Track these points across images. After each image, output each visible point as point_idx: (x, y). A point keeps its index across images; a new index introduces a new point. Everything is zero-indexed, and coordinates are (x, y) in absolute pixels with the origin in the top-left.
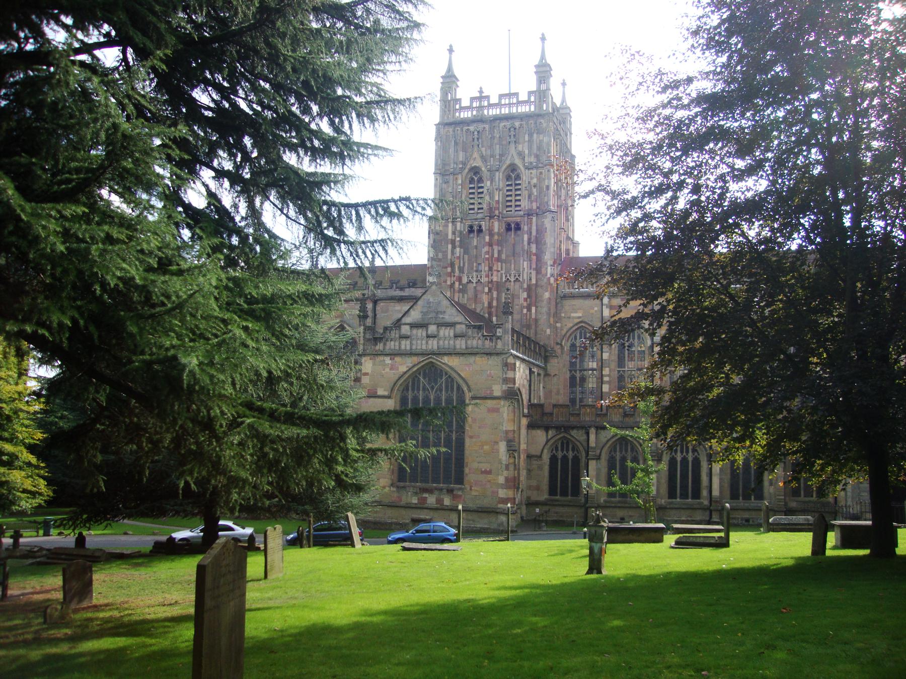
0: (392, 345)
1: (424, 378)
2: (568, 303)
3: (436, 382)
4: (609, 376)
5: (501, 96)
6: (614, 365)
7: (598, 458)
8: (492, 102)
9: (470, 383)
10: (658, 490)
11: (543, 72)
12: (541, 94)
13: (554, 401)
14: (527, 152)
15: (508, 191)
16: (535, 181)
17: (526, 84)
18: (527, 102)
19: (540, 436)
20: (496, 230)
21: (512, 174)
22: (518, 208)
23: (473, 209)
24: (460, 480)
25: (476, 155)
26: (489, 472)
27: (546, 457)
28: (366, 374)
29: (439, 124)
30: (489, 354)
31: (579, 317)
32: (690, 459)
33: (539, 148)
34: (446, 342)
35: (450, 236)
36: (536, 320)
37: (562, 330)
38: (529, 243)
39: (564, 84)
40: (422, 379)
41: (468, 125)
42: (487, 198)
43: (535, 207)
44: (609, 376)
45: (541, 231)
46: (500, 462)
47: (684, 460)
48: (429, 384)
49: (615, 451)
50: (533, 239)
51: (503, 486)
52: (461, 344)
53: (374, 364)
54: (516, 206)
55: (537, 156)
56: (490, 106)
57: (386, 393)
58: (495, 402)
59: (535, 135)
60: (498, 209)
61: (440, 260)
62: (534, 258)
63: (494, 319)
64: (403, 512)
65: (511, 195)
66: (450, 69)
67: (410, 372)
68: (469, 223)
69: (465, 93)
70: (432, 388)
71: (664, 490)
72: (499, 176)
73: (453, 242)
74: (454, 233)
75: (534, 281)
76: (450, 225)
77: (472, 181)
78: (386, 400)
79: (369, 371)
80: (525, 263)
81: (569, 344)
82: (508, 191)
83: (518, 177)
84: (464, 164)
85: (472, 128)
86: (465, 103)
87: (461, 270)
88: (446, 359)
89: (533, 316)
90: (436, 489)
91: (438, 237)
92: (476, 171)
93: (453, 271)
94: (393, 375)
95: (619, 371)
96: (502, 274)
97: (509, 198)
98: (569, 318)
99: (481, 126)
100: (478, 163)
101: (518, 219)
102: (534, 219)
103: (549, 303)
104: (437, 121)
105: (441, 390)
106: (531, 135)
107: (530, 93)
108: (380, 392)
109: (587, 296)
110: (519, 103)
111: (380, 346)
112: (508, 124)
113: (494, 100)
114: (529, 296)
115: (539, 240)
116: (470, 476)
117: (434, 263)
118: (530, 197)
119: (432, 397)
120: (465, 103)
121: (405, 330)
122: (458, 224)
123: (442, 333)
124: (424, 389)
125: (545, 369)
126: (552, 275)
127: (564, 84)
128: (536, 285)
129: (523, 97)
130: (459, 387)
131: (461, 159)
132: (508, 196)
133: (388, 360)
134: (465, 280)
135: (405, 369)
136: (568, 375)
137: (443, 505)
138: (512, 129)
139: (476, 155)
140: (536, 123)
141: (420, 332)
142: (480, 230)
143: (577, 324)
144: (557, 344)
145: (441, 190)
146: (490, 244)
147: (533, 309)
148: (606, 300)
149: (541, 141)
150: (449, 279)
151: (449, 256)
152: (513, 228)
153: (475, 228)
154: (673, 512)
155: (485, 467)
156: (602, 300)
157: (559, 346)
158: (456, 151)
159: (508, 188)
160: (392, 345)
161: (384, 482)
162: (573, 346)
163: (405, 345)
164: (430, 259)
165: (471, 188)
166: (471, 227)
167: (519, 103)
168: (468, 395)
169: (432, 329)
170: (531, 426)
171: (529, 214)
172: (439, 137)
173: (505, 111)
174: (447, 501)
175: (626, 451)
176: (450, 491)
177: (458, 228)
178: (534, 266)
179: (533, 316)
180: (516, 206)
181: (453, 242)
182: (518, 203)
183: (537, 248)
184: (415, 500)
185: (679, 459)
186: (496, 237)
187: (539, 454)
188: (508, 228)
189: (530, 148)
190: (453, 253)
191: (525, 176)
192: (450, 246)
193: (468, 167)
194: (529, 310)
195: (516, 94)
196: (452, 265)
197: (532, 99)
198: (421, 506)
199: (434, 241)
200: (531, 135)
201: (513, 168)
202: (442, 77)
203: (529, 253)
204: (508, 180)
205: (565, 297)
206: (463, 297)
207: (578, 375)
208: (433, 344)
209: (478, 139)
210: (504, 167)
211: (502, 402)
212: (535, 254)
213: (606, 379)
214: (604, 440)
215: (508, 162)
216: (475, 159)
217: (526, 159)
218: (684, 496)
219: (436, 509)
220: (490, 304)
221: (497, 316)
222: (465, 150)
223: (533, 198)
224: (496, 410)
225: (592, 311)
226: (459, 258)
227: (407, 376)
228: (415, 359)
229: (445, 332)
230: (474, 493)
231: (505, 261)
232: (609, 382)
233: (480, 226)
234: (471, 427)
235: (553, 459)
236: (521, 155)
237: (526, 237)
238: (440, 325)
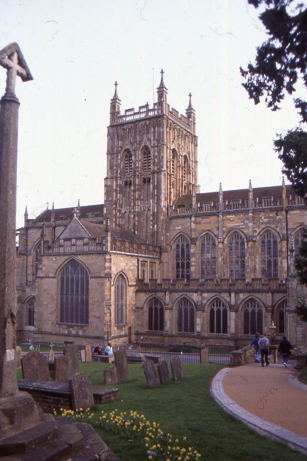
0: (56, 250)
1: (71, 267)
2: (174, 221)
3: (76, 269)
4: (194, 262)
5: (141, 108)
6: (197, 256)
7: (171, 309)
8: (135, 112)
9: (90, 269)
10: (202, 328)
11: (161, 91)
12: (160, 103)
13: (165, 277)
14: (152, 138)
15: (144, 161)
16: (156, 154)
17: (152, 99)
18: (153, 110)
19: (143, 297)
20: (137, 183)
21: (146, 151)
22: (149, 170)
23: (127, 172)
24: (87, 322)
25: (127, 142)
27: (146, 309)
29: (110, 126)
31: (180, 229)
32: (221, 310)
33: (159, 135)
34: (80, 248)
35: (114, 188)
36: (157, 232)
37: (171, 237)
38: (154, 189)
40: (70, 268)
41: (124, 126)
42: (133, 167)
43: (156, 169)
44: (194, 262)
45: (159, 182)
47: (218, 311)
48: (73, 270)
49: (182, 305)
50: (155, 186)
54: (149, 169)
55: (158, 141)
56: (135, 114)
57: (53, 276)
58: (102, 279)
59: (156, 128)
60: (138, 171)
61: (110, 201)
62: (156, 197)
63: (136, 232)
65: (145, 163)
67: (64, 265)
68: (125, 180)
70: (75, 272)
71: (207, 326)
72: (139, 152)
73: (116, 191)
74: (117, 185)
75: (156, 210)
76: (115, 182)
77: (126, 157)
78: (53, 279)
80: (151, 201)
81: (175, 245)
82: (144, 161)
83: (149, 153)
84: (121, 147)
85: (125, 127)
87: (121, 206)
89: (155, 230)
90: (76, 326)
91: (109, 189)
92: (128, 151)
93: (116, 207)
94: (56, 266)
95: (202, 259)
96: (141, 207)
97: (145, 165)
98: (175, 230)
101: (149, 176)
102: (156, 175)
103: (162, 222)
104: (108, 125)
105: (79, 274)
106: (154, 128)
107: (155, 104)
109: (184, 217)
111: (51, 251)
112: (143, 123)
113: (137, 110)
114: (154, 218)
115: (158, 187)
116: (91, 320)
117: (107, 203)
118: (154, 163)
119: (75, 277)
120: (122, 113)
122: (119, 181)
123: (78, 243)
124: (71, 273)
125: (160, 259)
126: (164, 207)
128: (157, 212)
129: (151, 107)
130: (86, 272)
131: (120, 145)
132: (144, 163)
134: (123, 211)
136: (175, 262)
137: (79, 335)
138: (145, 126)
139: (127, 142)
140: (157, 121)
143: (178, 234)
144: (168, 245)
145: (111, 162)
146: (134, 191)
147: (156, 226)
148: (193, 219)
149: (160, 131)
150: (114, 211)
151: (114, 199)
152: (146, 181)
153: (128, 183)
154: (211, 340)
155: (97, 314)
156: (191, 218)
157: (168, 246)
158: (118, 141)
159: (144, 159)
162: (178, 246)
164: (105, 201)
165: (126, 161)
166: (126, 182)
168: (90, 276)
170: (137, 292)
171: (153, 173)
172: (109, 134)
173: (143, 116)
174: (81, 333)
175: (188, 305)
176: (82, 327)
177: (118, 183)
178: (156, 202)
179: (155, 230)
180: (149, 169)
181: (116, 191)
182: (149, 167)
183: (157, 191)
184: (66, 332)
185: (215, 310)
186: (137, 187)
187: (142, 307)
188: (145, 182)
189: (154, 136)
190: (116, 196)
192: (114, 193)
193: (124, 149)
194: (153, 226)
196: (116, 204)
197: (156, 107)
198: (69, 335)
199: (107, 191)
200: (154, 128)
201: (146, 148)
203: (153, 194)
204: (144, 154)
205: (172, 218)
206: (122, 221)
207: (180, 262)
209: (129, 133)
210: (142, 147)
212: (157, 195)
213: (193, 264)
214: (175, 299)
215: (143, 145)
216: (127, 145)
218: (218, 331)
220: (134, 224)
221: (137, 230)
222: (122, 139)
223: (156, 163)
225: (186, 226)
226: (119, 199)
227: (62, 266)
228: (66, 257)
231: (143, 200)
232: (194, 266)
233: (131, 181)
234: (91, 293)
235: (150, 310)
236: (149, 140)
237: (151, 186)
238: (77, 239)
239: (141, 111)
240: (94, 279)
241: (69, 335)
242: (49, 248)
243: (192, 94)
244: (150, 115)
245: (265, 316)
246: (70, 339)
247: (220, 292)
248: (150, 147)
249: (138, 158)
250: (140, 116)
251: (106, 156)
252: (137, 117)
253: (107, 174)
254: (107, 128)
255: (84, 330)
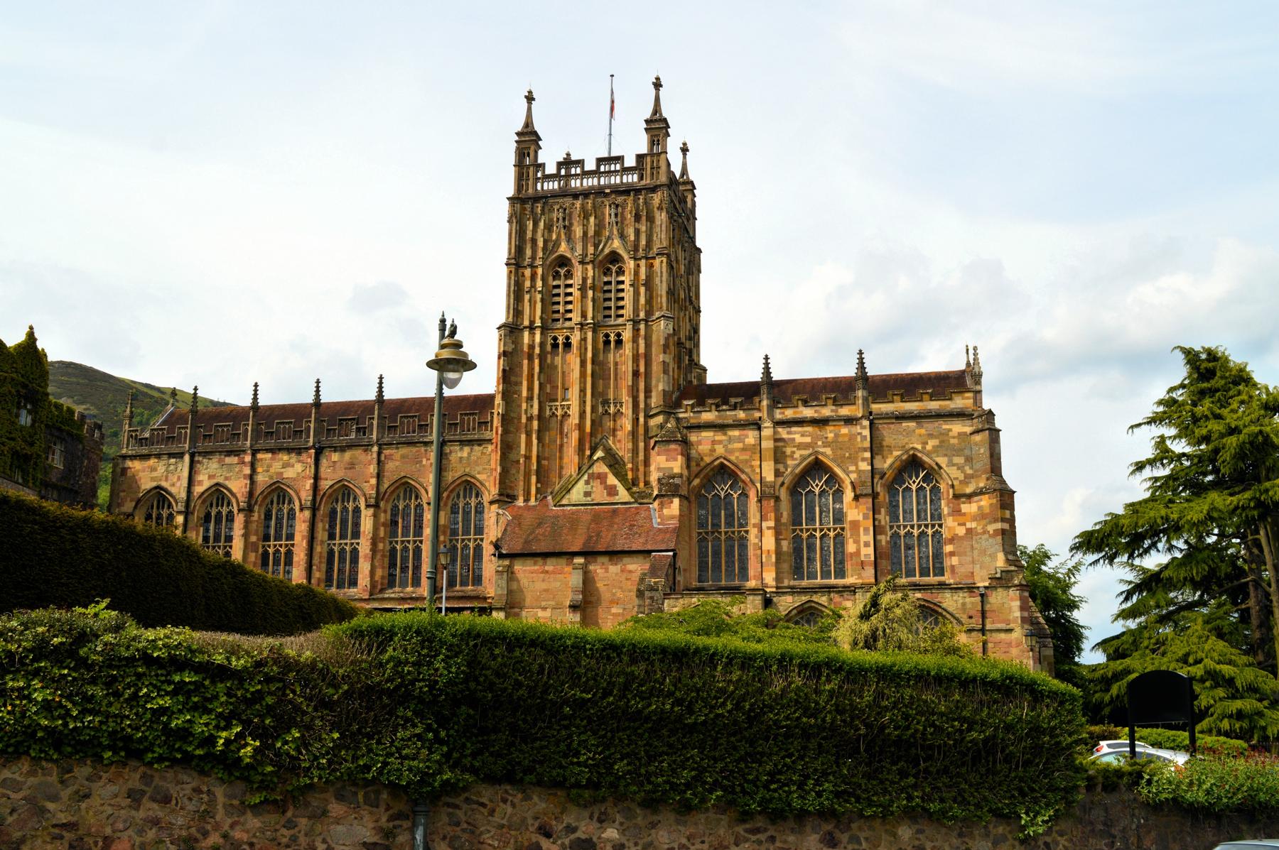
5: (600, 161)
11: (657, 127)
17: (633, 144)
39: (685, 150)
66: (528, 123)
69: (549, 157)
86: (551, 169)
104: (511, 191)
107: (640, 158)
110: (626, 170)
120: (551, 169)
127: (685, 150)
129: (630, 162)
167: (626, 170)
195: (619, 159)
202: (518, 134)
239: (602, 169)
243: (689, 146)
244: (573, 185)
250: (582, 184)
251: (505, 270)
253: (508, 318)
254: (508, 202)
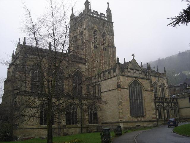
5: (101, 13)
24: (143, 113)
26: (150, 111)
28: (122, 81)
30: (147, 79)
46: (152, 108)
47: (159, 110)
51: (154, 114)
52: (141, 76)
53: (123, 79)
56: (98, 15)
64: (133, 123)
79: (122, 80)
88: (139, 79)
90: (140, 116)
92: (95, 31)
99: (97, 19)
100: (97, 29)
102: (111, 48)
105: (137, 88)
108: (125, 87)
110: (104, 17)
111: (123, 73)
120: (92, 11)
121: (129, 69)
133: (126, 78)
135: (130, 81)
141: (132, 71)
142: (97, 48)
155: (149, 109)
160: (126, 74)
161: (129, 115)
163: (129, 74)
166: (94, 46)
169: (135, 70)
176: (143, 116)
184: (136, 120)
191: (107, 37)
198: (137, 122)
201: (104, 33)
208: (135, 75)
211: (151, 92)
217: (108, 32)
219: (141, 122)
224: (149, 94)
229: (137, 72)
230: (148, 117)
236: (107, 31)
240: (146, 92)
241: (137, 122)
242: (124, 71)
245: (171, 112)
246: (138, 124)
247: (160, 103)
248: (107, 33)
249: (99, 37)
252: (99, 17)
255: (144, 118)
